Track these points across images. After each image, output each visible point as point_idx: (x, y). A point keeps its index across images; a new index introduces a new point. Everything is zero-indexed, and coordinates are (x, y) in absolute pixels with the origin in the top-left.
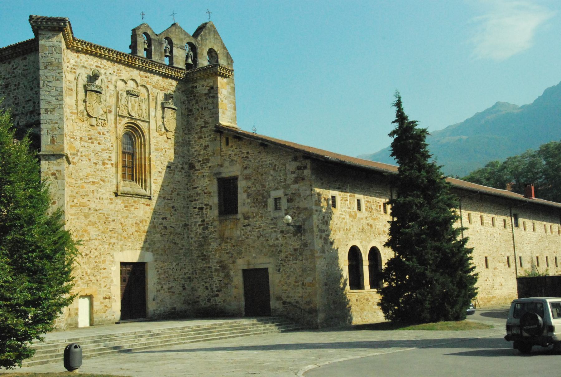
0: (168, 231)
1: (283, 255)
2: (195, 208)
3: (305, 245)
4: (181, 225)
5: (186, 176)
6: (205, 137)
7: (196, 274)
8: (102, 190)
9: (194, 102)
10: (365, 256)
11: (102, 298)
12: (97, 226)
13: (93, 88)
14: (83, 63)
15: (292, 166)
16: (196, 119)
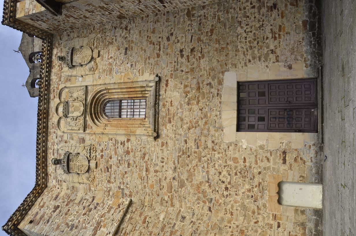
2: (164, 6)
4: (189, 22)
5: (134, 22)
8: (154, 158)
11: (283, 167)
12: (192, 170)
14: (53, 170)
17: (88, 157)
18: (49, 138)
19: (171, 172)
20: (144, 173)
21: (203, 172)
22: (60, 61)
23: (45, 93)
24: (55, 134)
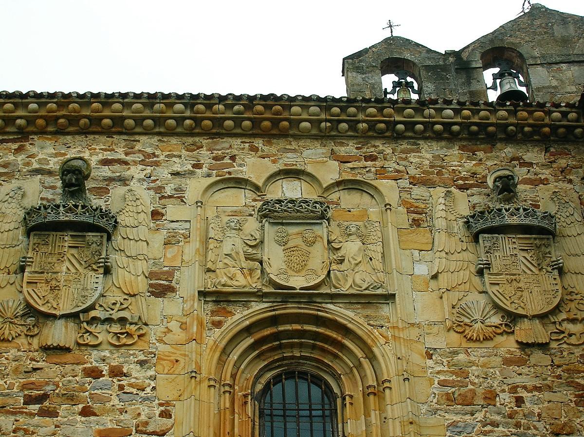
14: (40, 161)
17: (93, 314)
18: (174, 141)
22: (495, 181)
23: (359, 122)
24: (190, 167)
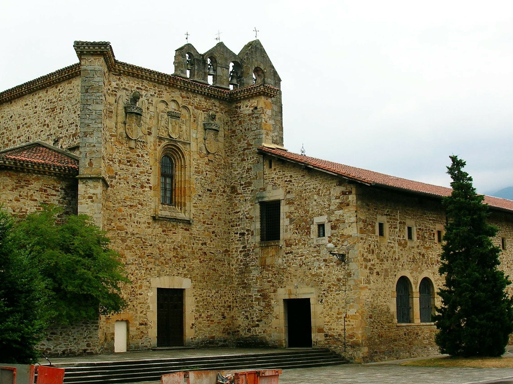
0: (208, 257)
1: (325, 285)
2: (237, 233)
3: (349, 275)
5: (227, 200)
6: (248, 160)
7: (237, 302)
9: (237, 122)
10: (416, 287)
11: (138, 323)
12: (133, 250)
13: (133, 110)
15: (336, 190)
16: (239, 141)
18: (151, 83)
19: (131, 230)
20: (129, 203)
21: (133, 260)
